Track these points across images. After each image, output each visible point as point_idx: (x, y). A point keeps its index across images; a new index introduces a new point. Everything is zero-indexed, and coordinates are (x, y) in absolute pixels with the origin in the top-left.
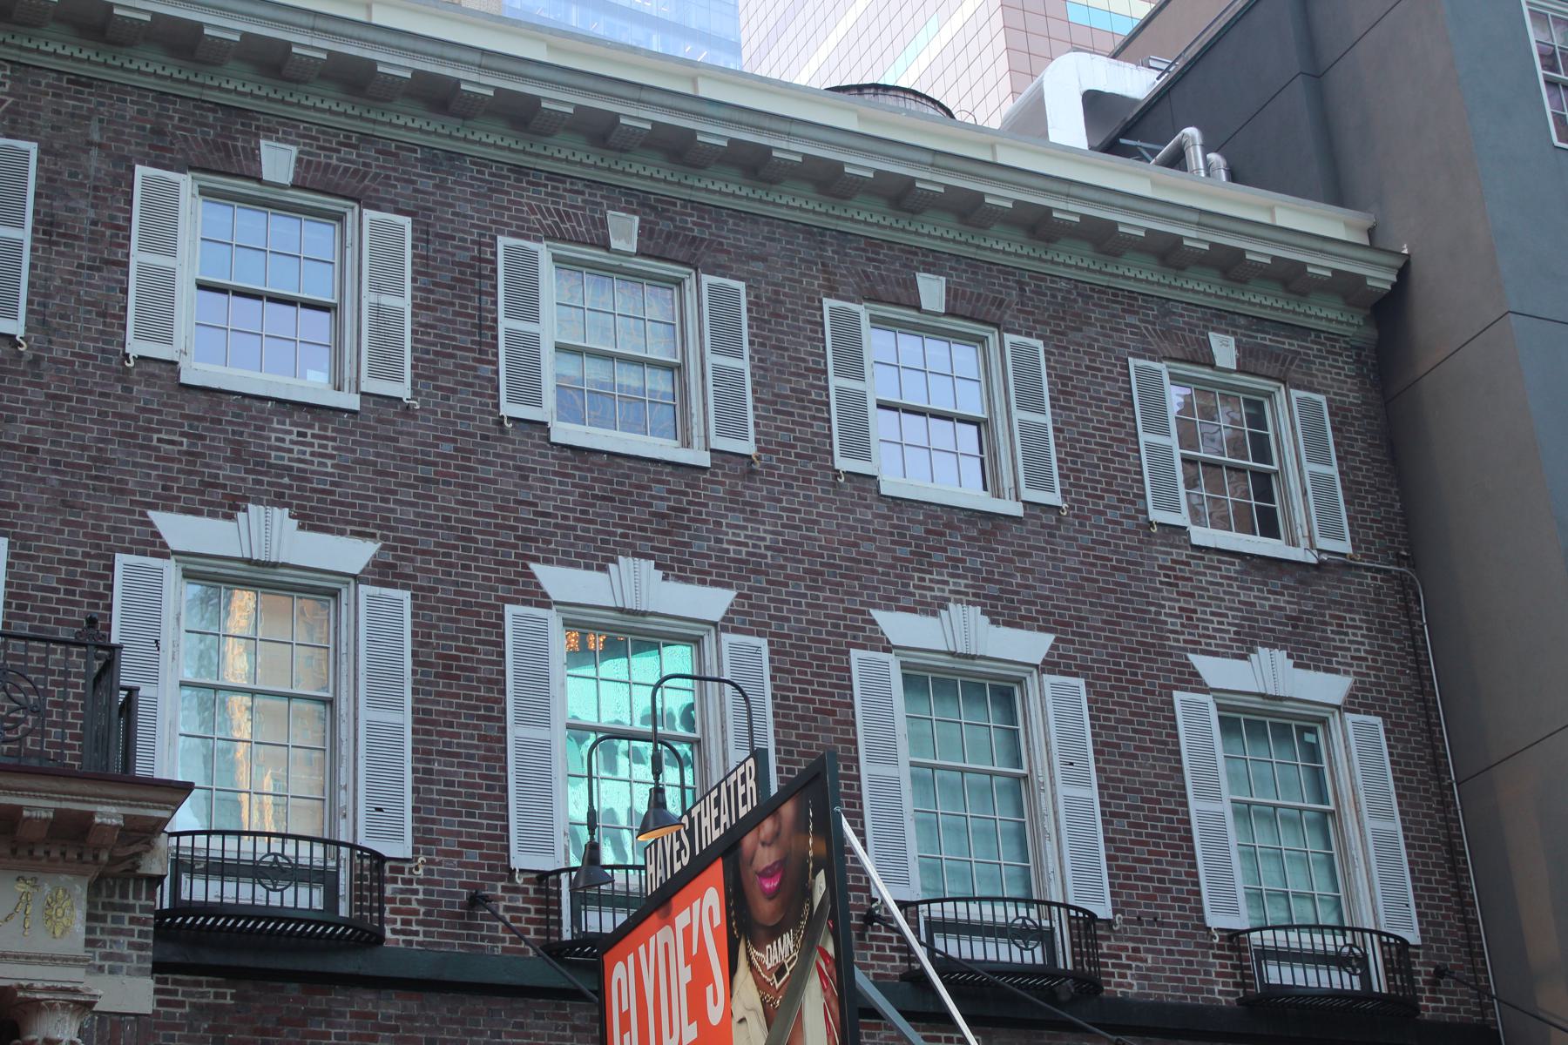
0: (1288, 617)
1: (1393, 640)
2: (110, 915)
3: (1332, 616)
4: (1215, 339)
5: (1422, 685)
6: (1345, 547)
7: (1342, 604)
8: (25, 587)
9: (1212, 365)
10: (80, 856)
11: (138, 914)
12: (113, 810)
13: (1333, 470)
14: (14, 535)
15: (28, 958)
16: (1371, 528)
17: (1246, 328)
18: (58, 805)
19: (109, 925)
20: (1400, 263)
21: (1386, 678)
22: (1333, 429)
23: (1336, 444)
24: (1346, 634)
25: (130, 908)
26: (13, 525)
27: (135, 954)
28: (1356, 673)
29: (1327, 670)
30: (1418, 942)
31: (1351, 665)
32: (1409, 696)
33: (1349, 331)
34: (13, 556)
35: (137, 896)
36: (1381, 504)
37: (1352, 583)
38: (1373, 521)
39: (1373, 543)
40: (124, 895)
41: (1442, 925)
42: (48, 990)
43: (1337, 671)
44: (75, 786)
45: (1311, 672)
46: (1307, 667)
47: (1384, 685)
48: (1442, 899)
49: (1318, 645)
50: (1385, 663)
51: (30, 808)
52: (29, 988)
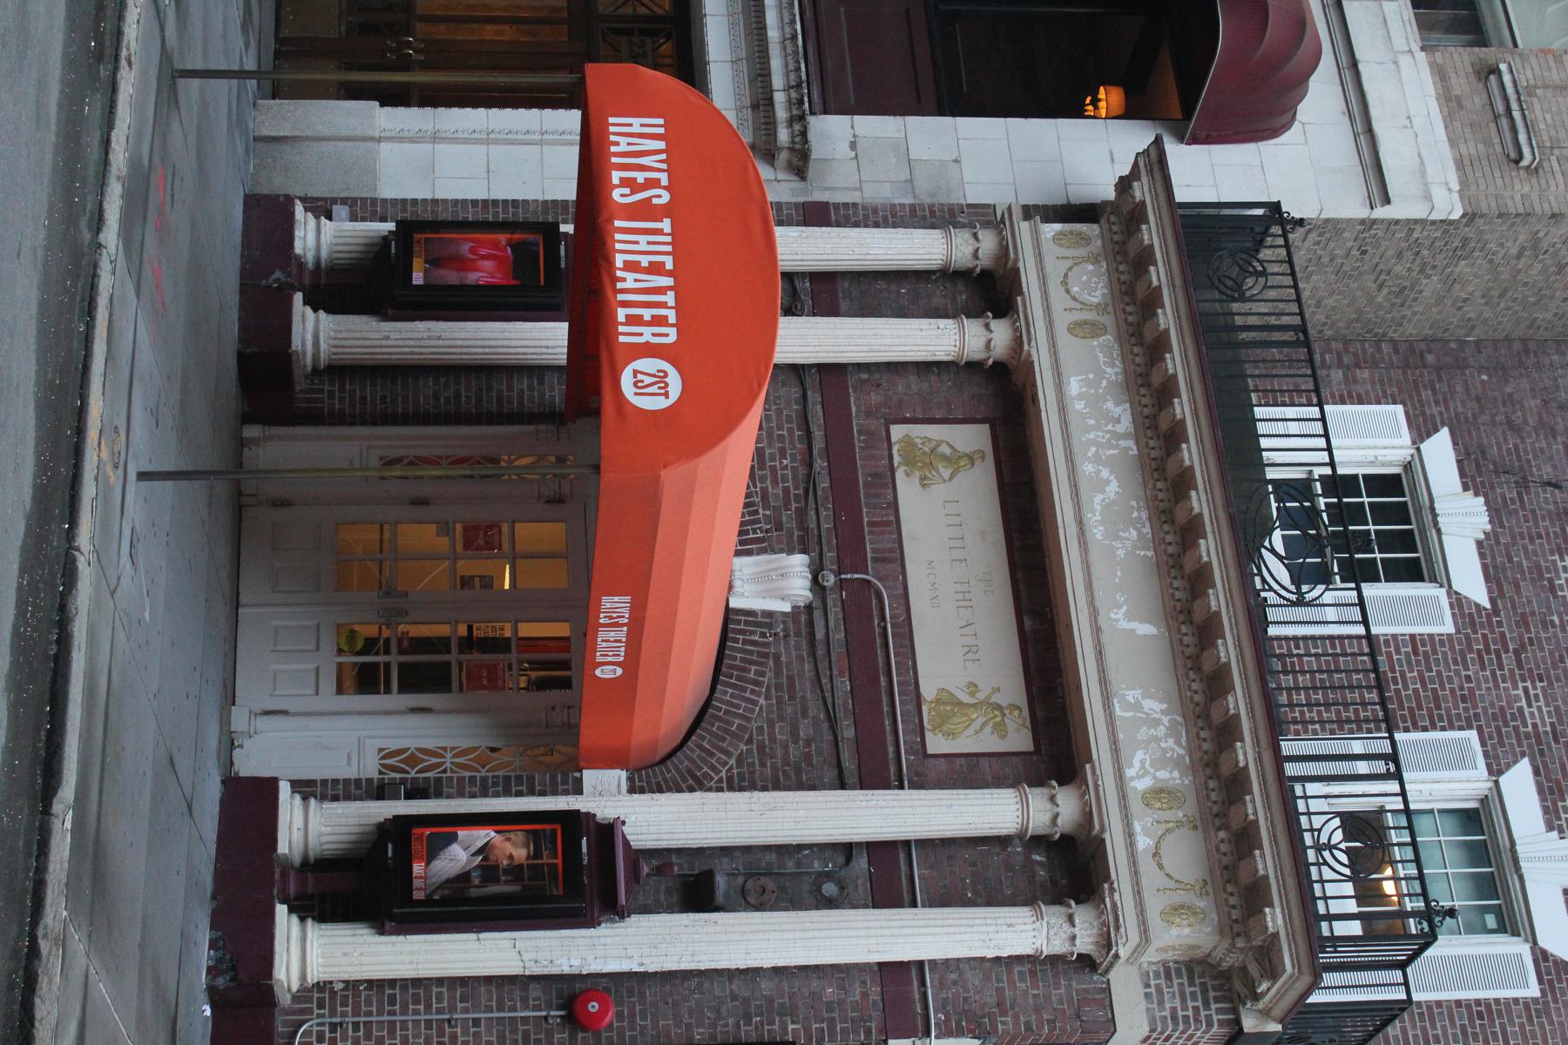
2: (1197, 989)
8: (1500, 1015)
10: (1236, 921)
11: (1203, 1013)
12: (1280, 921)
14: (1546, 1003)
15: (1138, 893)
18: (1273, 881)
19: (1188, 990)
25: (1207, 1005)
26: (1555, 1001)
27: (1167, 1013)
34: (1527, 1003)
35: (1219, 1011)
40: (1217, 1000)
42: (1114, 905)
44: (1291, 883)
51: (1263, 855)
52: (1112, 890)
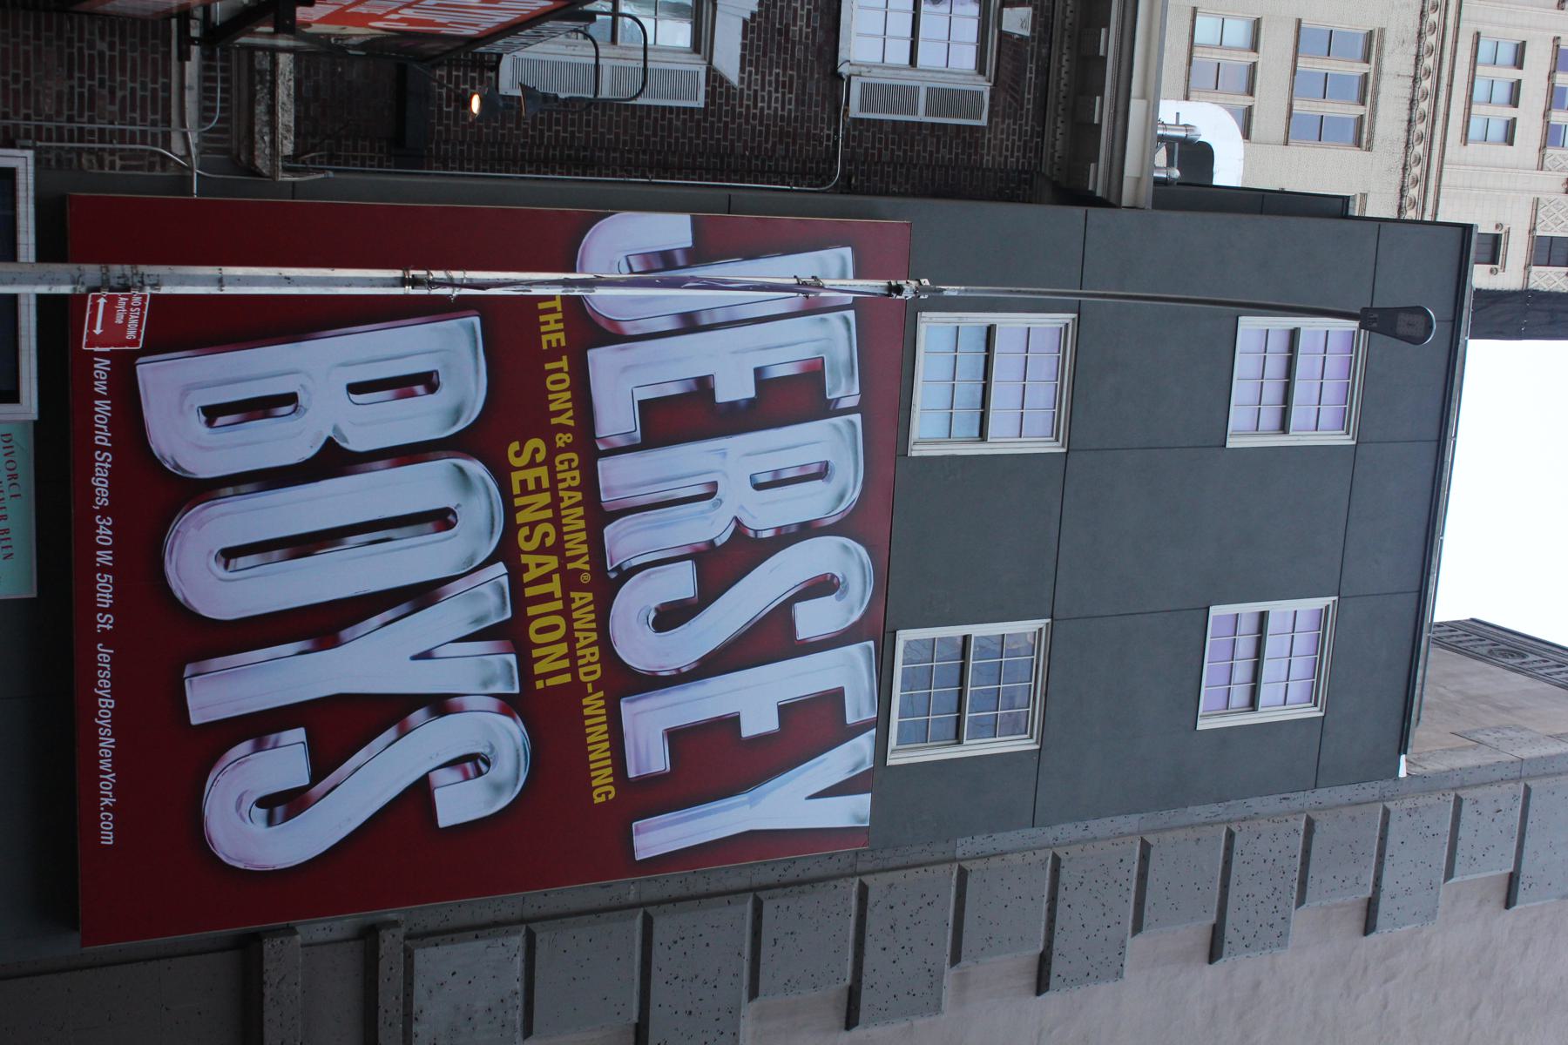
0: (787, 26)
1: (774, 144)
3: (791, 77)
4: (1025, 13)
5: (735, 172)
6: (855, 111)
7: (804, 93)
9: (1003, 5)
13: (921, 117)
16: (873, 147)
17: (1039, 53)
20: (1113, 200)
21: (740, 125)
22: (958, 126)
23: (945, 125)
24: (777, 91)
28: (742, 90)
29: (743, 57)
30: (502, 92)
31: (749, 88)
32: (725, 148)
33: (1046, 170)
36: (895, 169)
37: (823, 109)
38: (880, 151)
39: (860, 146)
41: (518, 128)
43: (742, 70)
45: (739, 39)
46: (744, 36)
47: (733, 122)
48: (542, 132)
49: (765, 55)
50: (754, 128)
